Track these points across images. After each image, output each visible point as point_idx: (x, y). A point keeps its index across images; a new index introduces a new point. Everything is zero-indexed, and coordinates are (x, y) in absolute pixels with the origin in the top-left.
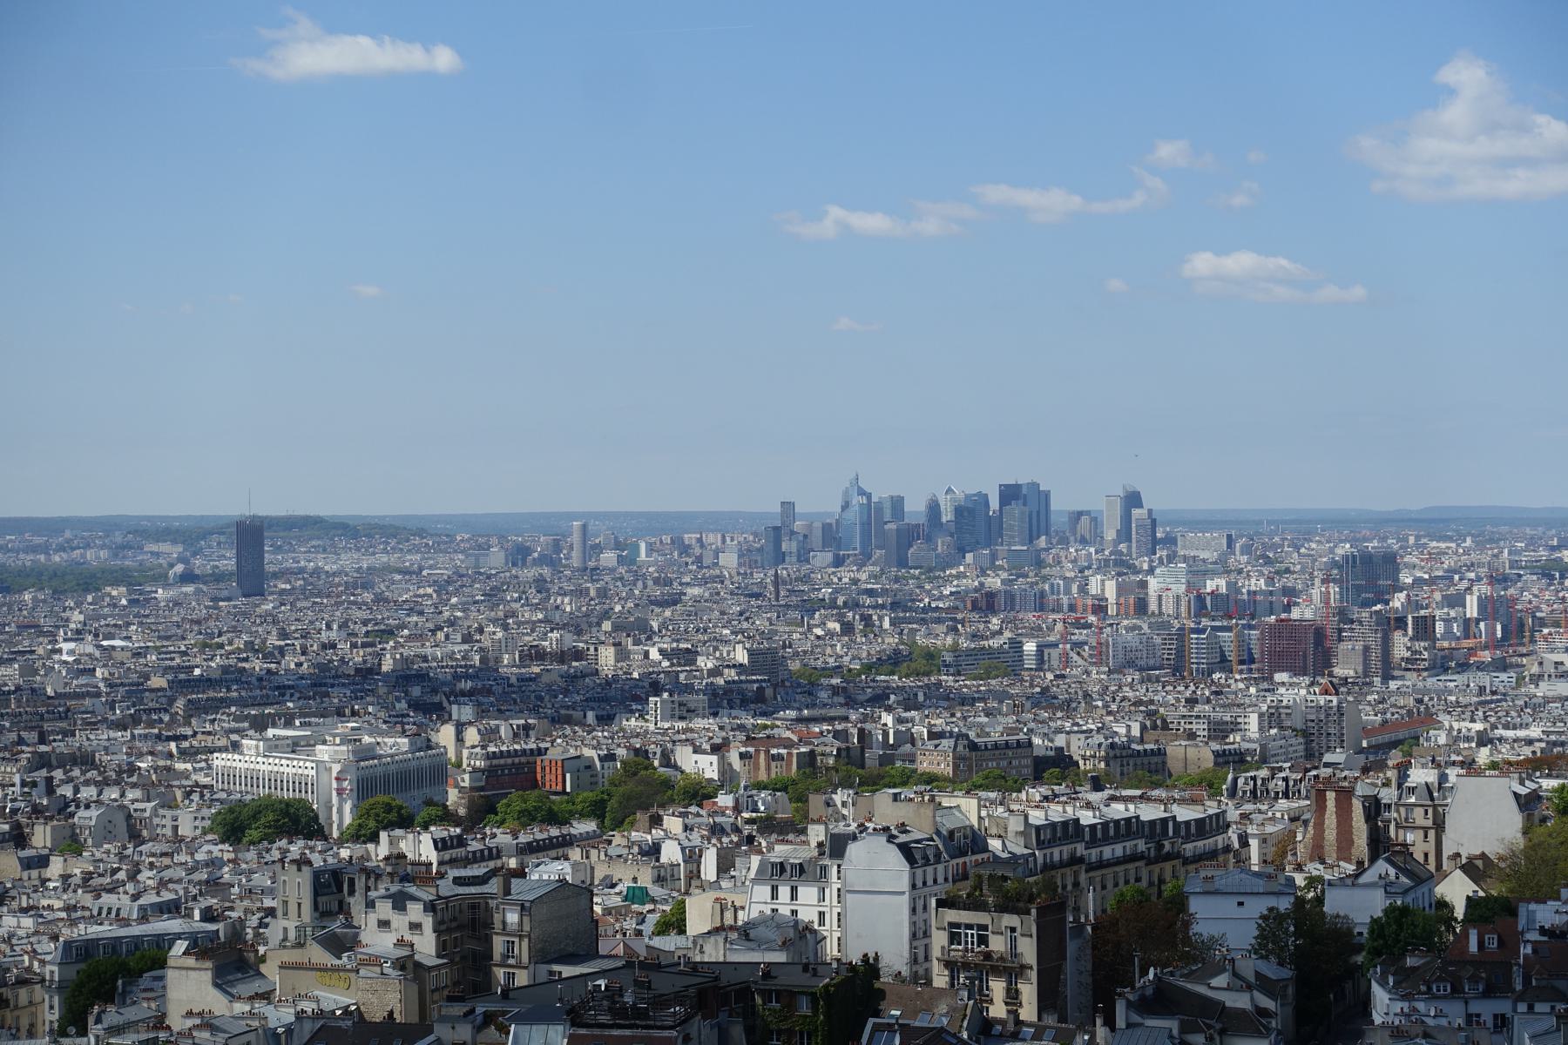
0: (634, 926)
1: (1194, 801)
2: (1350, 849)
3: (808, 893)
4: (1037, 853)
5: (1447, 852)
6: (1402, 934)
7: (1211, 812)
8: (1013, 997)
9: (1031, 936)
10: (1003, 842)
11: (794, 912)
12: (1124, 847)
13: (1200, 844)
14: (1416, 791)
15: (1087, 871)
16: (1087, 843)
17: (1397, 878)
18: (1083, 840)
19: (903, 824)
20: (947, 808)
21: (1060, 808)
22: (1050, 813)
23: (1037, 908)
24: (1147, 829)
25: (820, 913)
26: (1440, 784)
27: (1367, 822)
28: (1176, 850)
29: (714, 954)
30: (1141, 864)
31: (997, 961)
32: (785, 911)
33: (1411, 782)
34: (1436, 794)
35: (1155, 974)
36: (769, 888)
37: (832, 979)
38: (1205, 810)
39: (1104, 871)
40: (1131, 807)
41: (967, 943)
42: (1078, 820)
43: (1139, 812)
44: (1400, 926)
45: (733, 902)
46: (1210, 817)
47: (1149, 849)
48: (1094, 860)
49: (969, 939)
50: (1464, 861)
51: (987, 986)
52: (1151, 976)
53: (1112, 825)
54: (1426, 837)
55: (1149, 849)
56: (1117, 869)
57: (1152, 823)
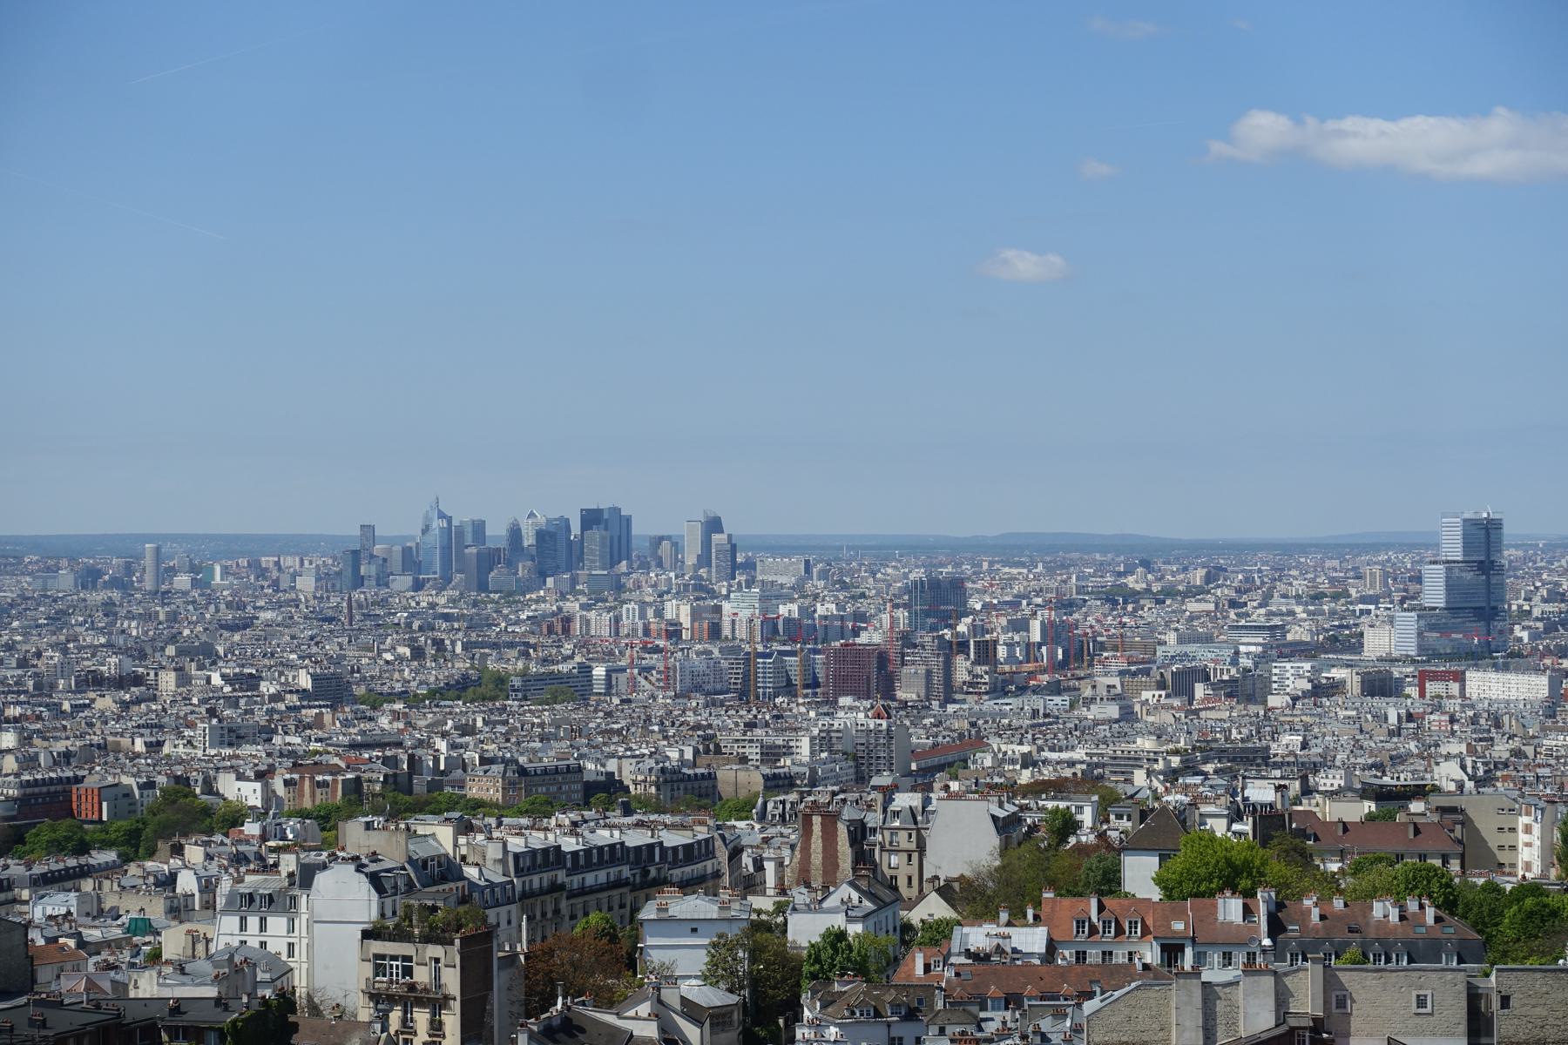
0: (128, 959)
1: (683, 827)
2: (835, 873)
3: (277, 924)
4: (515, 880)
5: (927, 875)
6: (838, 959)
7: (700, 837)
8: (436, 1027)
9: (455, 967)
10: (480, 870)
11: (263, 944)
12: (608, 874)
13: (688, 869)
14: (901, 815)
15: (568, 898)
16: (569, 869)
17: (861, 902)
18: (564, 867)
19: (374, 853)
20: (421, 836)
21: (541, 835)
22: (529, 840)
23: (461, 939)
24: (632, 856)
25: (289, 944)
26: (924, 808)
27: (851, 846)
28: (662, 876)
29: (149, 989)
30: (625, 890)
31: (421, 992)
32: (254, 943)
33: (893, 807)
34: (919, 818)
35: (563, 1004)
36: (238, 918)
37: (241, 1014)
38: (694, 835)
39: (586, 898)
40: (616, 833)
41: (391, 974)
42: (560, 846)
43: (624, 838)
44: (836, 950)
45: (205, 934)
46: (699, 842)
47: (634, 875)
48: (575, 886)
49: (394, 971)
50: (942, 884)
51: (411, 1018)
52: (559, 1006)
53: (595, 851)
54: (910, 860)
55: (634, 875)
56: (600, 895)
57: (638, 849)
